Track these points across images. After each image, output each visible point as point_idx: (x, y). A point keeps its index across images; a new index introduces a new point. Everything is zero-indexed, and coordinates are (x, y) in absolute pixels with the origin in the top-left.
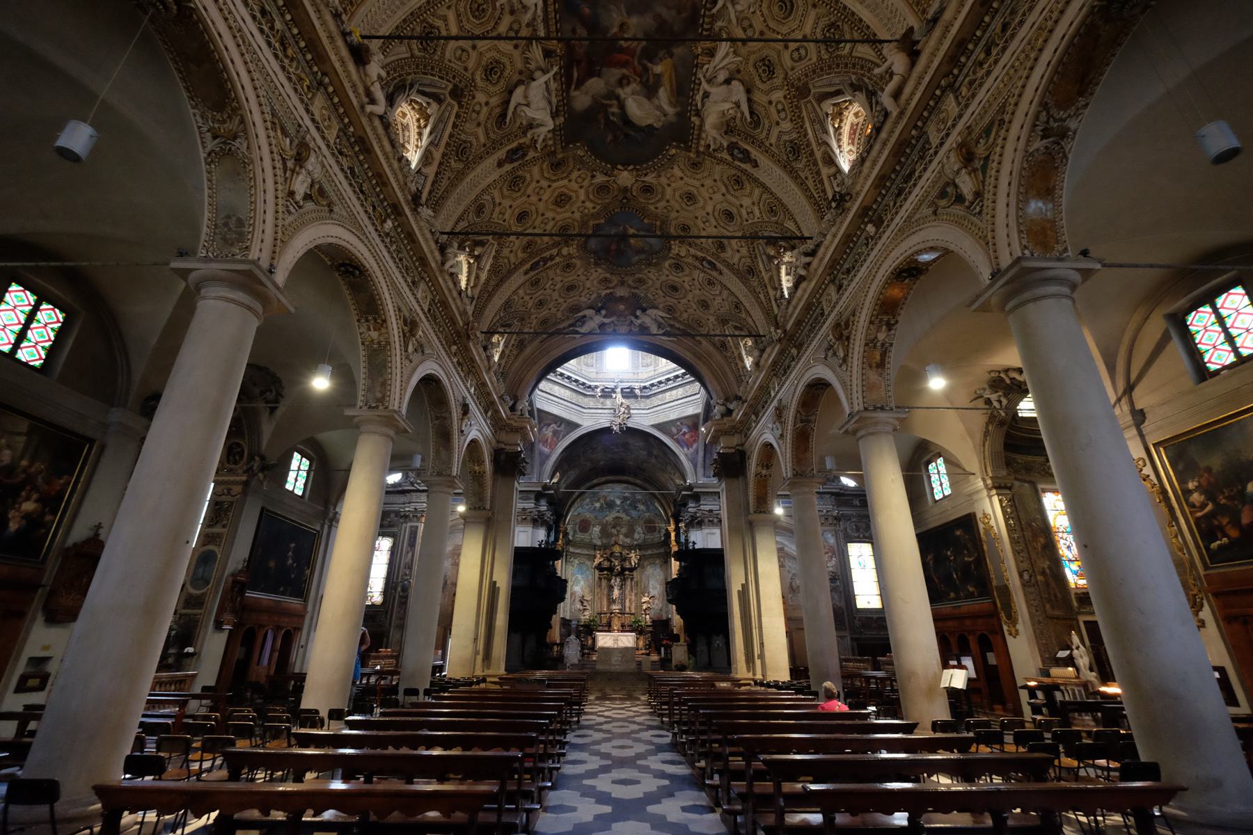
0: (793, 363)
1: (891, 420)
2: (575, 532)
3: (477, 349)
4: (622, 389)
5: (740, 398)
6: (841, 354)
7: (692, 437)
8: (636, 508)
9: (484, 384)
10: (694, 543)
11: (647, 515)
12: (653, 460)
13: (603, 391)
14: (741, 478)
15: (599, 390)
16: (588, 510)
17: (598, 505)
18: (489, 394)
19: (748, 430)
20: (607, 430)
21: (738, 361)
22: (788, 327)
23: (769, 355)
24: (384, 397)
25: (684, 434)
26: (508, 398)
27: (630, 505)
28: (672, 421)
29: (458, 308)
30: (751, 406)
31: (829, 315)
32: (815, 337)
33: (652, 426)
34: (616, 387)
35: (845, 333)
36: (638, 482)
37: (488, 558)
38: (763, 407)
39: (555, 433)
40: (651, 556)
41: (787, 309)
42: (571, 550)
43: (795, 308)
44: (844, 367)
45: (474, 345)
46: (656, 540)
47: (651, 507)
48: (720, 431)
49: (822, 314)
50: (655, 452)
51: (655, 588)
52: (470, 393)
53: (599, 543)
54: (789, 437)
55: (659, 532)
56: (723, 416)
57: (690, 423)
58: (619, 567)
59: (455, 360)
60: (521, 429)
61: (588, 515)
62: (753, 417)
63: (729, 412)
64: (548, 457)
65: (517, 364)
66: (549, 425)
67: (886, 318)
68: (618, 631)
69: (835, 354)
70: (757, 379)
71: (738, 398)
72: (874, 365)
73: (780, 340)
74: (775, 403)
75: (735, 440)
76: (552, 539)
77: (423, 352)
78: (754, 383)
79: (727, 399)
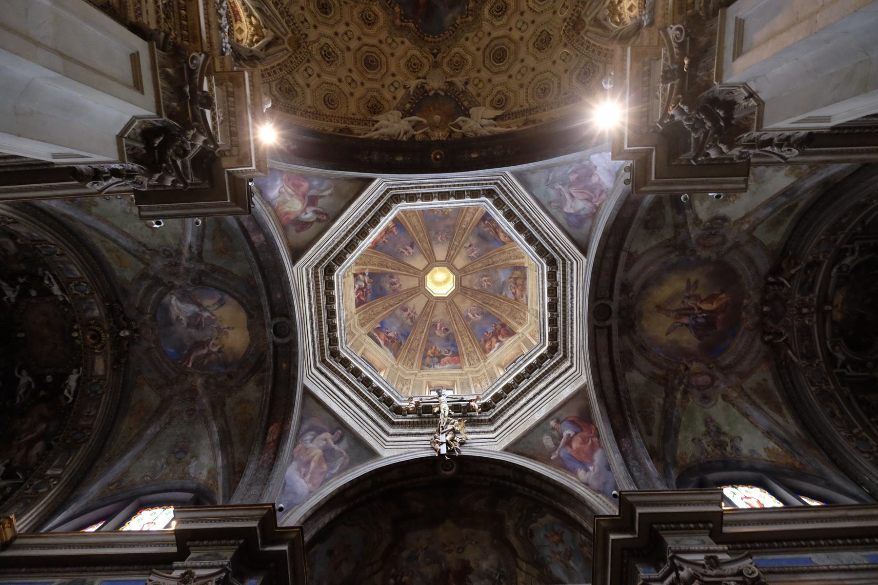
7: (584, 442)
33: (507, 450)
39: (328, 454)
66: (320, 431)
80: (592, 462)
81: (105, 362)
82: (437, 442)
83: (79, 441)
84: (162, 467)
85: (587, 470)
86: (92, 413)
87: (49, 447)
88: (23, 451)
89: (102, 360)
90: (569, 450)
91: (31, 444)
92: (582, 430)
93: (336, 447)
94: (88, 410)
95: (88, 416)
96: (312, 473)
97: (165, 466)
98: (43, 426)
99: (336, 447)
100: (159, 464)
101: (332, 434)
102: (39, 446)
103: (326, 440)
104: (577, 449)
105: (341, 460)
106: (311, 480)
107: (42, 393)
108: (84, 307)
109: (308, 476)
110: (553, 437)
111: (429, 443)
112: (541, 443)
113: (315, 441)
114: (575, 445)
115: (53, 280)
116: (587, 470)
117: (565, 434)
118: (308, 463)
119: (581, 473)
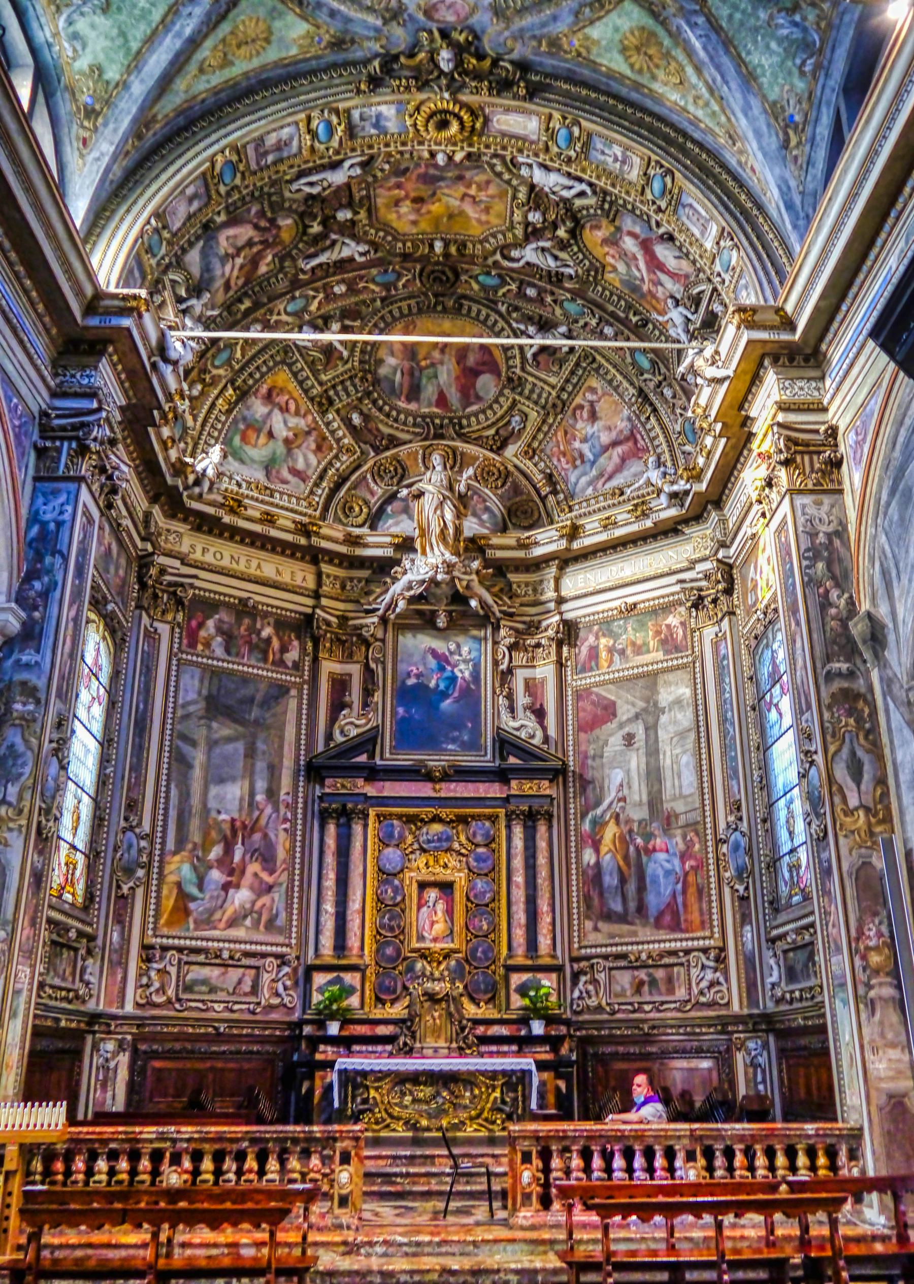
81: (507, 110)
83: (669, 185)
84: (796, 24)
86: (619, 154)
87: (671, 238)
88: (663, 278)
89: (503, 117)
91: (655, 264)
94: (610, 160)
95: (624, 162)
97: (797, 18)
98: (629, 244)
100: (785, 32)
102: (663, 252)
107: (561, 233)
108: (373, 131)
115: (314, 178)
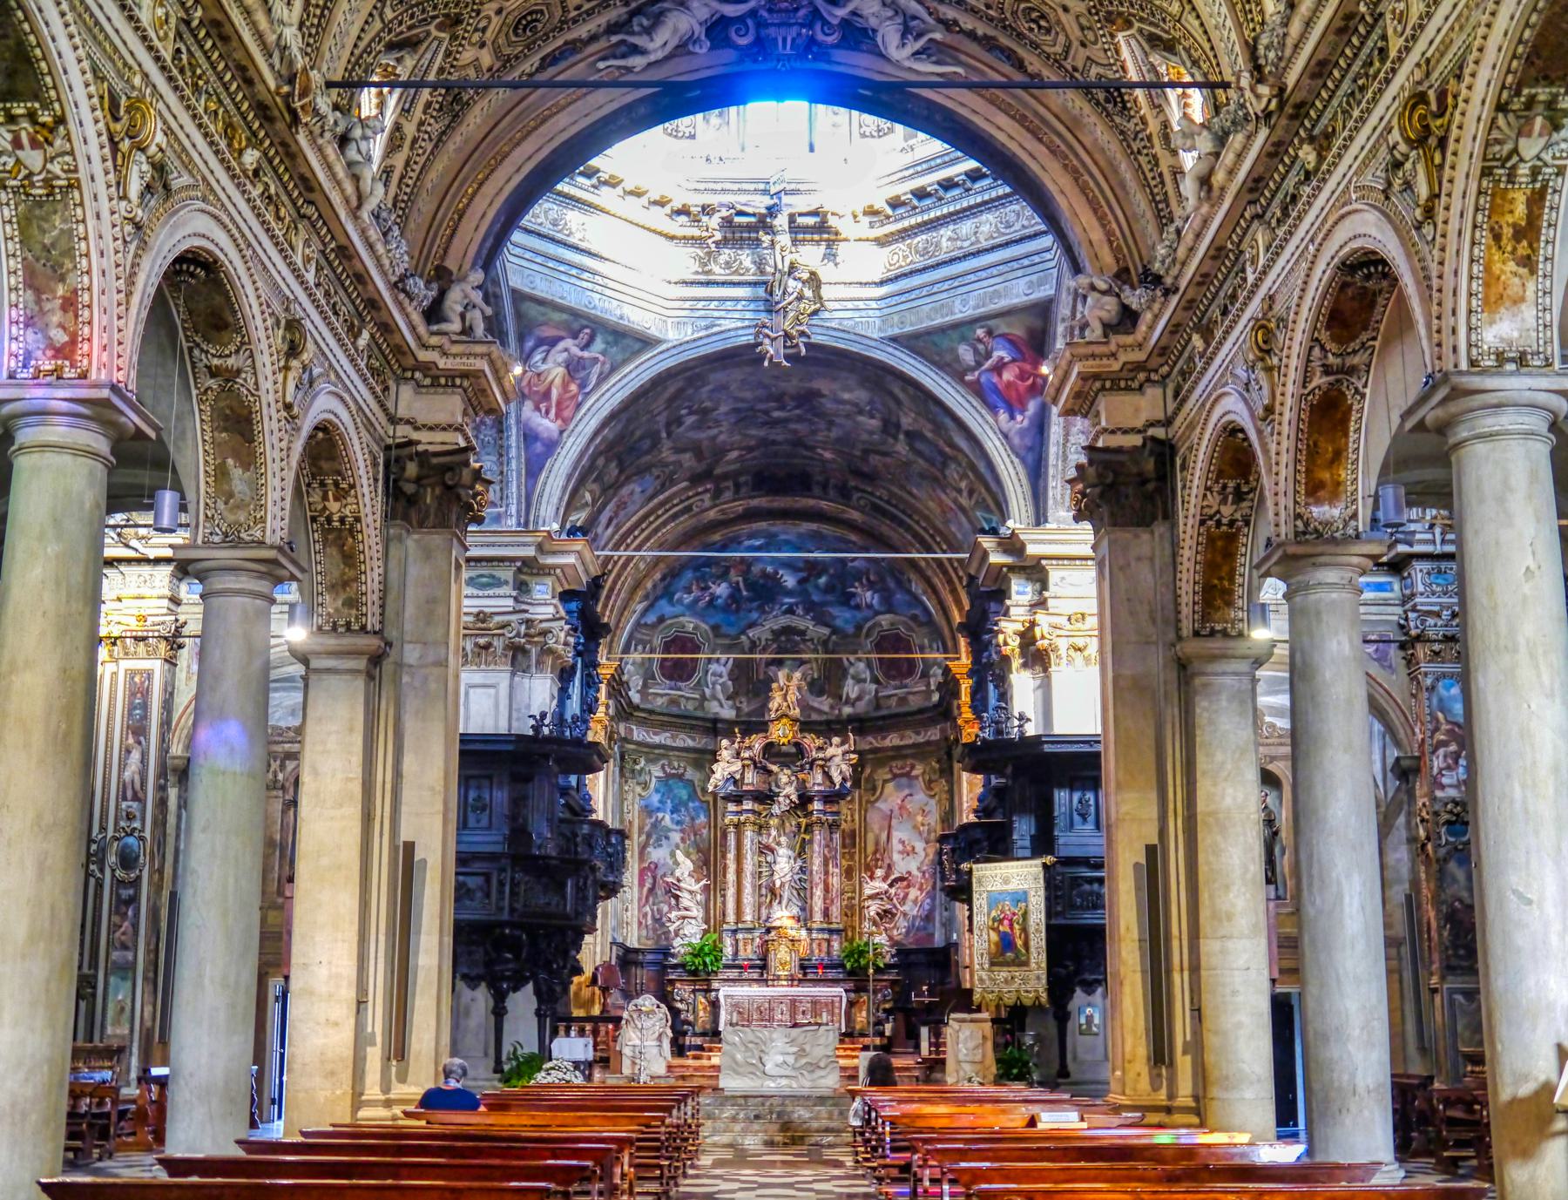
0: (1307, 190)
1: (1542, 398)
2: (648, 677)
3: (320, 149)
4: (792, 218)
5: (1158, 280)
6: (1423, 190)
7: (1022, 376)
8: (847, 600)
9: (345, 252)
10: (1022, 717)
11: (885, 620)
12: (901, 447)
13: (727, 223)
14: (1160, 528)
15: (714, 221)
16: (692, 606)
17: (721, 590)
18: (361, 278)
19: (1184, 374)
20: (742, 357)
21: (1158, 148)
22: (1291, 79)
23: (1240, 156)
24: (73, 342)
25: (999, 368)
26: (417, 285)
27: (829, 589)
28: (956, 326)
29: (259, 36)
30: (1190, 305)
31: (1400, 60)
32: (1362, 119)
33: (894, 339)
34: (772, 211)
35: (1435, 124)
36: (855, 515)
37: (383, 774)
38: (1225, 312)
39: (574, 368)
40: (898, 753)
41: (1286, 23)
42: (639, 734)
43: (1308, 24)
44: (1428, 230)
45: (313, 141)
46: (915, 703)
47: (899, 596)
48: (1096, 377)
49: (1383, 52)
50: (907, 421)
51: (909, 852)
52: (299, 277)
53: (728, 713)
54: (1287, 413)
55: (925, 675)
56: (1109, 328)
57: (1018, 331)
58: (790, 790)
59: (256, 192)
60: (465, 375)
61: (690, 623)
62: (1197, 341)
63: (1128, 318)
64: (552, 446)
65: (439, 166)
66: (553, 342)
67: (1543, 94)
68: (792, 979)
69: (1408, 186)
70: (1206, 222)
71: (1152, 279)
72: (1507, 232)
73: (1268, 115)
74: (1254, 307)
75: (1145, 406)
76: (574, 706)
77: (166, 187)
78: (1198, 236)
79: (1122, 275)
80: (1023, 411)
82: (767, 336)
85: (1012, 418)
90: (995, 379)
92: (1024, 360)
93: (586, 354)
96: (559, 403)
99: (586, 354)
101: (575, 337)
103: (566, 350)
104: (1009, 384)
105: (596, 369)
106: (557, 415)
109: (553, 411)
110: (976, 351)
111: (752, 331)
112: (953, 351)
113: (550, 358)
114: (1008, 376)
116: (1012, 418)
117: (997, 354)
118: (546, 395)
119: (1003, 416)
